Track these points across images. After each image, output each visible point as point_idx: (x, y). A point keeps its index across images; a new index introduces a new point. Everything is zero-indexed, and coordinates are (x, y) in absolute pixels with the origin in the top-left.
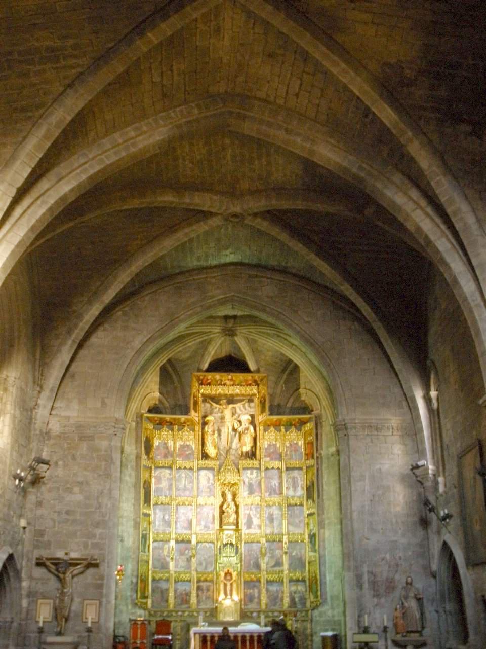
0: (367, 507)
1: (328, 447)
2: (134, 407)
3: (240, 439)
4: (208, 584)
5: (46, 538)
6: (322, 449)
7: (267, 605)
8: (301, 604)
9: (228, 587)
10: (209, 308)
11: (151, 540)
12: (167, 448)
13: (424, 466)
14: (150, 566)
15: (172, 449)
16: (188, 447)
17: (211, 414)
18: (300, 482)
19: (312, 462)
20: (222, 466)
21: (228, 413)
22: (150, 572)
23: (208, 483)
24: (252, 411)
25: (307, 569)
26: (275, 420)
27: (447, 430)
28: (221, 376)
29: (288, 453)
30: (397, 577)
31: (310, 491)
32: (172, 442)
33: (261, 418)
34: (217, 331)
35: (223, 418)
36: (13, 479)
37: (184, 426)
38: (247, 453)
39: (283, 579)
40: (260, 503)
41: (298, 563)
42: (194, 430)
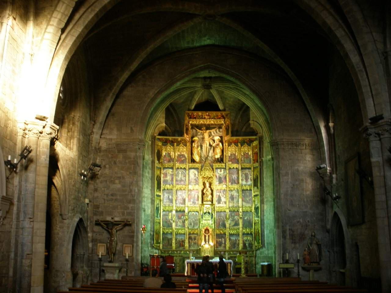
0: (289, 191)
1: (267, 155)
2: (150, 132)
3: (214, 151)
4: (195, 235)
5: (100, 209)
6: (263, 157)
7: (229, 248)
8: (249, 247)
9: (207, 238)
10: (194, 72)
11: (162, 211)
12: (170, 156)
13: (324, 167)
15: (173, 157)
16: (183, 156)
17: (196, 136)
18: (250, 177)
19: (257, 165)
20: (203, 167)
21: (206, 135)
22: (161, 229)
23: (195, 177)
24: (221, 134)
26: (235, 139)
27: (339, 147)
28: (202, 113)
30: (306, 232)
32: (173, 153)
33: (226, 138)
34: (199, 86)
35: (203, 138)
36: (79, 175)
37: (180, 143)
38: (218, 159)
40: (225, 189)
41: (248, 224)
42: (186, 145)
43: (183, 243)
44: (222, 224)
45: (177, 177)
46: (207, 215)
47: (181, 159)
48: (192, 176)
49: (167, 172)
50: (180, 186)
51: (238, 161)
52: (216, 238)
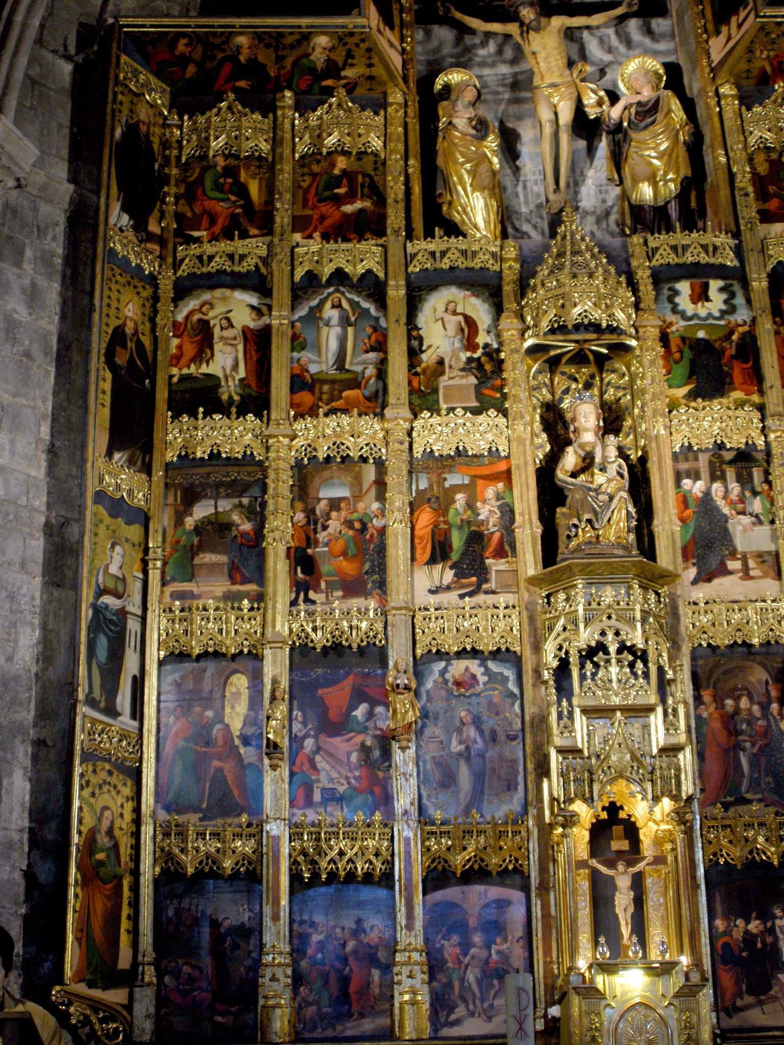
3: (617, 159)
4: (494, 892)
9: (623, 901)
11: (154, 654)
20: (540, 260)
21: (545, 47)
22: (147, 831)
23: (471, 345)
35: (521, 86)
37: (329, 91)
40: (760, 442)
42: (380, 105)
43: (369, 974)
44: (754, 761)
45: (306, 356)
46: (614, 670)
47: (346, 200)
48: (439, 337)
49: (214, 316)
50: (331, 423)
52: (711, 917)
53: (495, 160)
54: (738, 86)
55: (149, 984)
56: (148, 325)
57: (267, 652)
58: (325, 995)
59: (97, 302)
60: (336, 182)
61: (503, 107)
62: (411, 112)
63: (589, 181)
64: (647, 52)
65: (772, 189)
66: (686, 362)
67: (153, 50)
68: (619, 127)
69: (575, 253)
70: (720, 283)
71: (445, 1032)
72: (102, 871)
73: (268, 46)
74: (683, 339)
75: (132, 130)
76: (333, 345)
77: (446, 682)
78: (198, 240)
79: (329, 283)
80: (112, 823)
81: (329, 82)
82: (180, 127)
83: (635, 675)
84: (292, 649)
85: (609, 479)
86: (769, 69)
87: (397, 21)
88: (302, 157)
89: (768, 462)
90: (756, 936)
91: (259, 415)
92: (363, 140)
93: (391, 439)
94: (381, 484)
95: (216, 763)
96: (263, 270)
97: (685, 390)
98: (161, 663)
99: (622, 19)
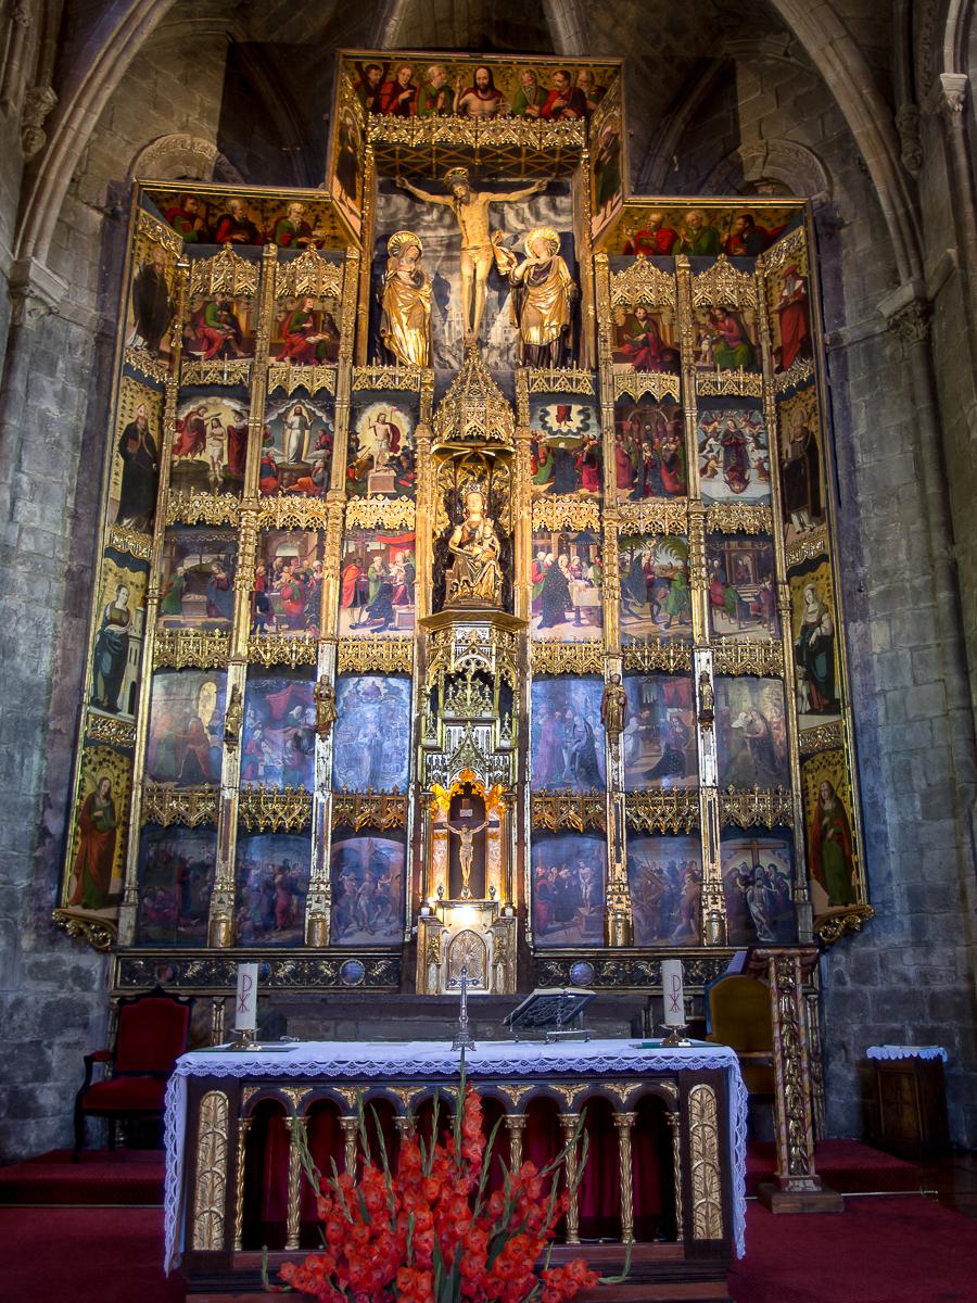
4: (384, 844)
9: (466, 853)
14: (138, 770)
18: (755, 455)
21: (473, 217)
22: (137, 794)
23: (394, 447)
25: (796, 783)
28: (450, 71)
29: (705, 346)
31: (800, 486)
35: (453, 246)
37: (303, 246)
38: (545, 350)
39: (697, 819)
40: (596, 526)
42: (340, 260)
43: (290, 899)
45: (273, 450)
46: (469, 691)
47: (307, 335)
48: (372, 442)
50: (287, 501)
51: (677, 356)
53: (428, 306)
54: (609, 255)
55: (132, 905)
56: (157, 422)
57: (231, 668)
58: (258, 913)
59: (112, 407)
60: (302, 318)
61: (438, 263)
62: (364, 267)
63: (497, 324)
64: (550, 223)
65: (626, 337)
66: (548, 465)
67: (171, 209)
68: (521, 284)
69: (472, 381)
70: (580, 408)
71: (343, 941)
72: (99, 824)
73: (256, 208)
74: (548, 448)
75: (149, 273)
76: (294, 443)
77: (358, 692)
78: (198, 358)
79: (293, 396)
80: (109, 789)
81: (303, 239)
82: (189, 269)
83: (483, 695)
84: (249, 665)
85: (484, 551)
86: (632, 243)
87: (359, 192)
88: (281, 297)
89: (602, 542)
90: (564, 881)
91: (235, 493)
92: (326, 286)
93: (331, 514)
94: (321, 548)
95: (190, 746)
96: (246, 384)
97: (545, 487)
98: (154, 673)
99: (536, 195)
